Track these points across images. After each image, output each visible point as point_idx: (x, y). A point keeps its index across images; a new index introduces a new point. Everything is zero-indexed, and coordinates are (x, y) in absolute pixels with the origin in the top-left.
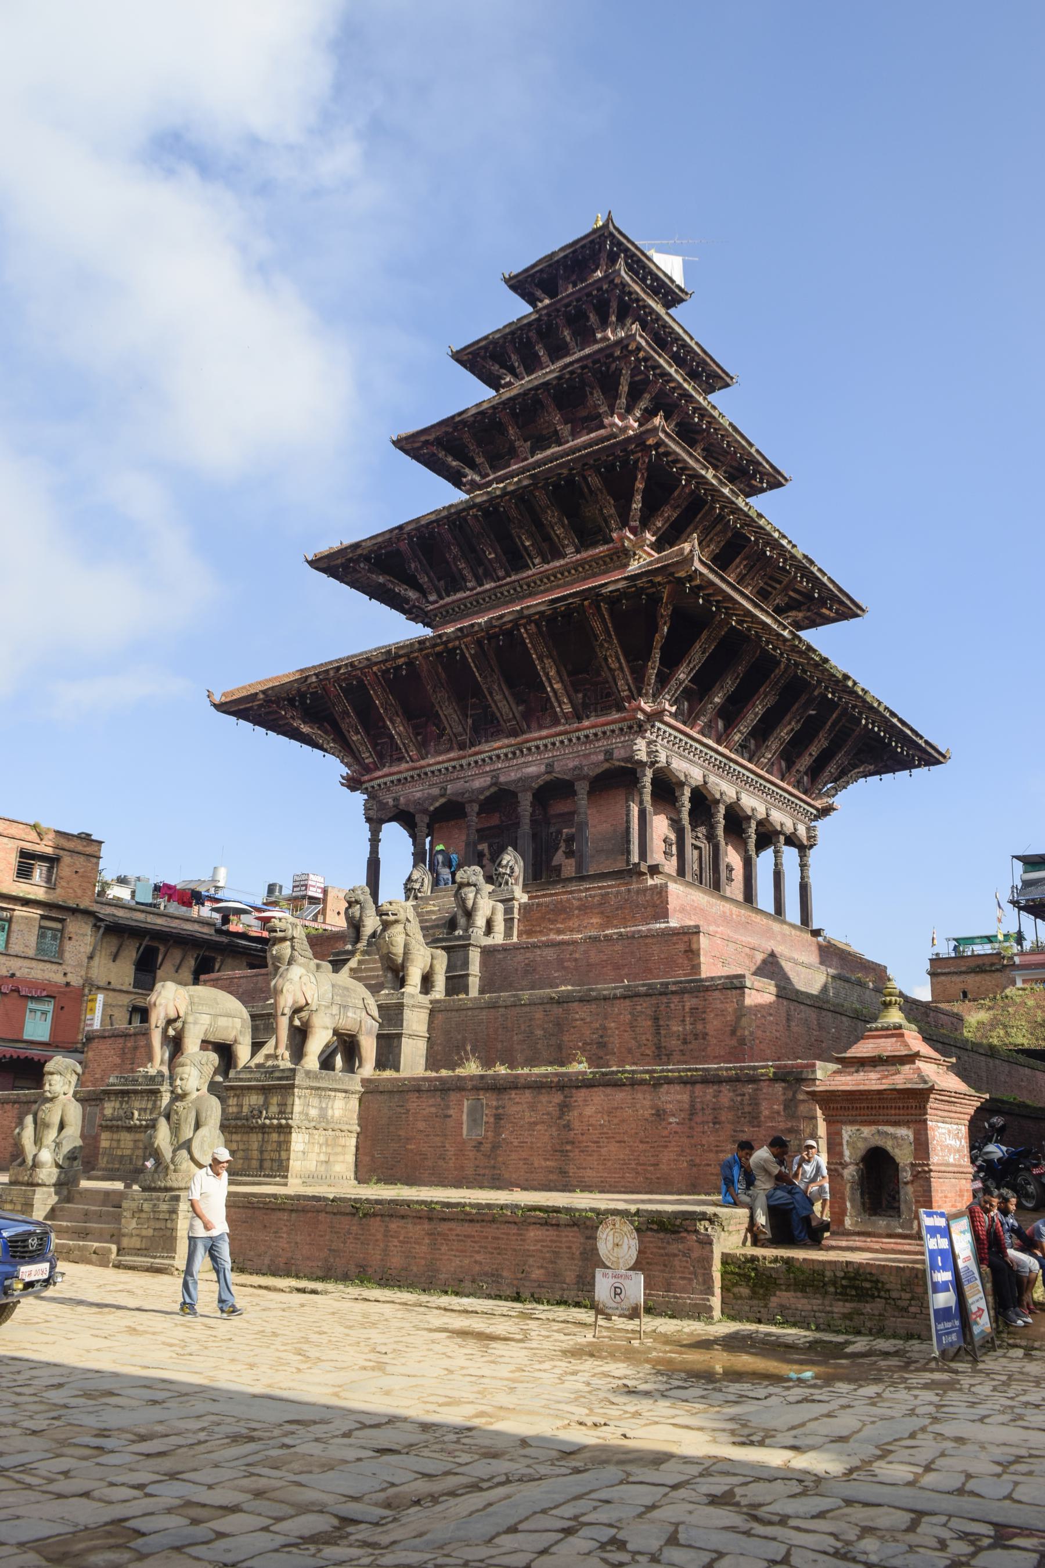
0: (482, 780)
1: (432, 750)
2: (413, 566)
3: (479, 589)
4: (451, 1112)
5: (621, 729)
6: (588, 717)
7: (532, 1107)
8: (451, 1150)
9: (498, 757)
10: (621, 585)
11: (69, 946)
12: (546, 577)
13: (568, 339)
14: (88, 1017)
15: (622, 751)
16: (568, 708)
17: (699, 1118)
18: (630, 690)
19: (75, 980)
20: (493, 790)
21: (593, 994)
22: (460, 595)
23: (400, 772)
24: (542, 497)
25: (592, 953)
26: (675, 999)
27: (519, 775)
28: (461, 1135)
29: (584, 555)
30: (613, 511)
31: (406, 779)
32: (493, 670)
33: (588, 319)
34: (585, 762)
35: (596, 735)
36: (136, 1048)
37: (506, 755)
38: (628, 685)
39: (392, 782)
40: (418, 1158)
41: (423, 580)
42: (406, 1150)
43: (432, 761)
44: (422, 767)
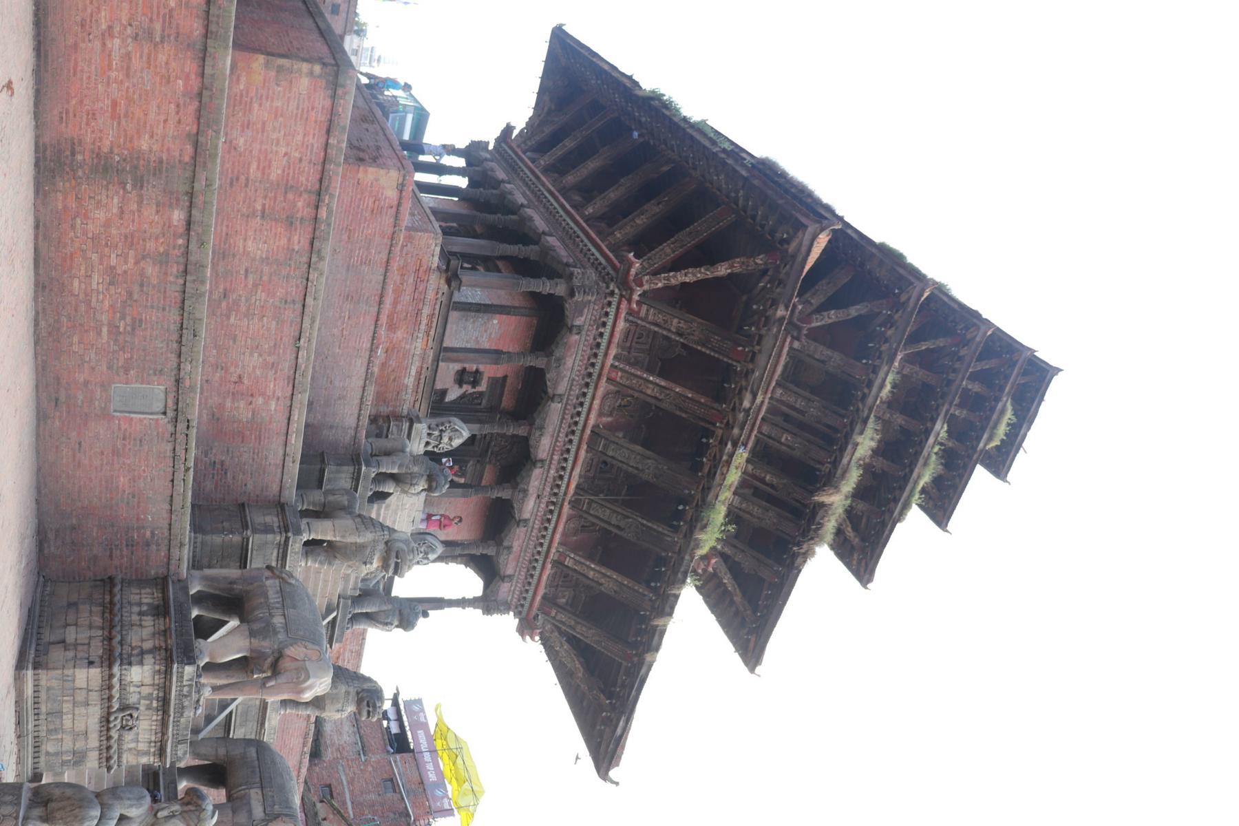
5: (525, 598)
9: (561, 477)
10: (619, 731)
18: (554, 618)
23: (606, 354)
27: (531, 490)
31: (595, 355)
34: (511, 557)
35: (532, 576)
36: (290, 222)
37: (558, 486)
38: (562, 622)
39: (601, 335)
41: (821, 351)
43: (597, 403)
44: (596, 388)
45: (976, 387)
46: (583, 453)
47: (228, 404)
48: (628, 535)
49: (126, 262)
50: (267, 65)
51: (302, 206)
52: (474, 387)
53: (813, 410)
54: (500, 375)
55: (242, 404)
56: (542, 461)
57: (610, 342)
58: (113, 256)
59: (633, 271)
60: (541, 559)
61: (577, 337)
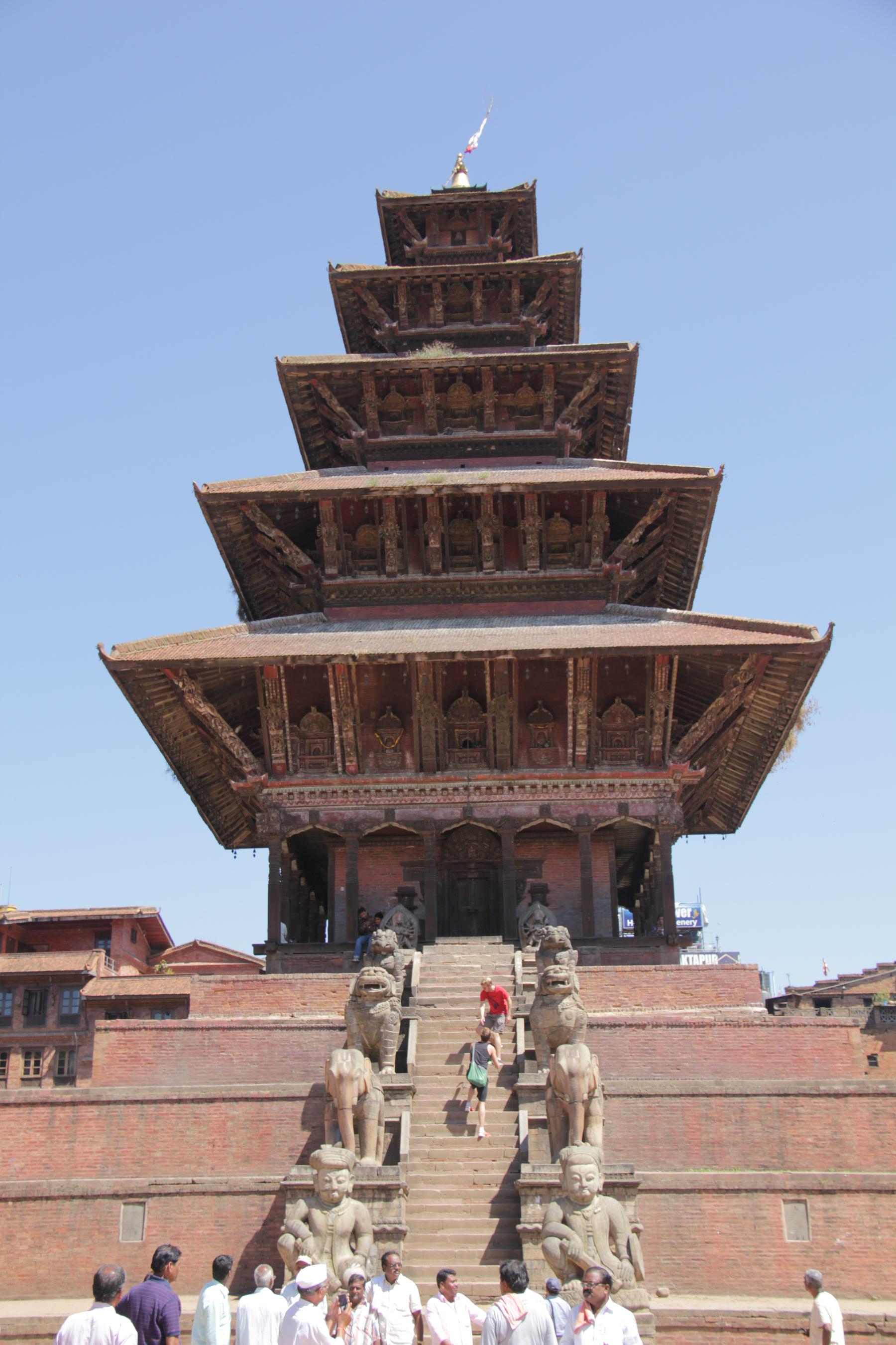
0: (449, 810)
1: (371, 765)
2: (324, 530)
3: (401, 577)
4: (765, 1213)
5: (644, 785)
9: (478, 788)
12: (500, 585)
13: (478, 304)
15: (640, 809)
16: (582, 751)
20: (464, 823)
21: (822, 1088)
22: (369, 577)
24: (531, 506)
27: (502, 813)
28: (782, 1239)
29: (554, 573)
30: (602, 538)
31: (334, 792)
32: (511, 696)
33: (509, 294)
35: (611, 785)
37: (489, 788)
39: (312, 793)
40: (724, 1265)
41: (329, 548)
42: (706, 1255)
45: (402, 304)
47: (234, 1150)
48: (512, 703)
49: (26, 1239)
51: (62, 1113)
52: (416, 894)
53: (390, 527)
54: (401, 870)
55: (233, 1139)
56: (465, 810)
57: (316, 784)
58: (21, 1248)
59: (241, 784)
60: (584, 782)
61: (321, 814)
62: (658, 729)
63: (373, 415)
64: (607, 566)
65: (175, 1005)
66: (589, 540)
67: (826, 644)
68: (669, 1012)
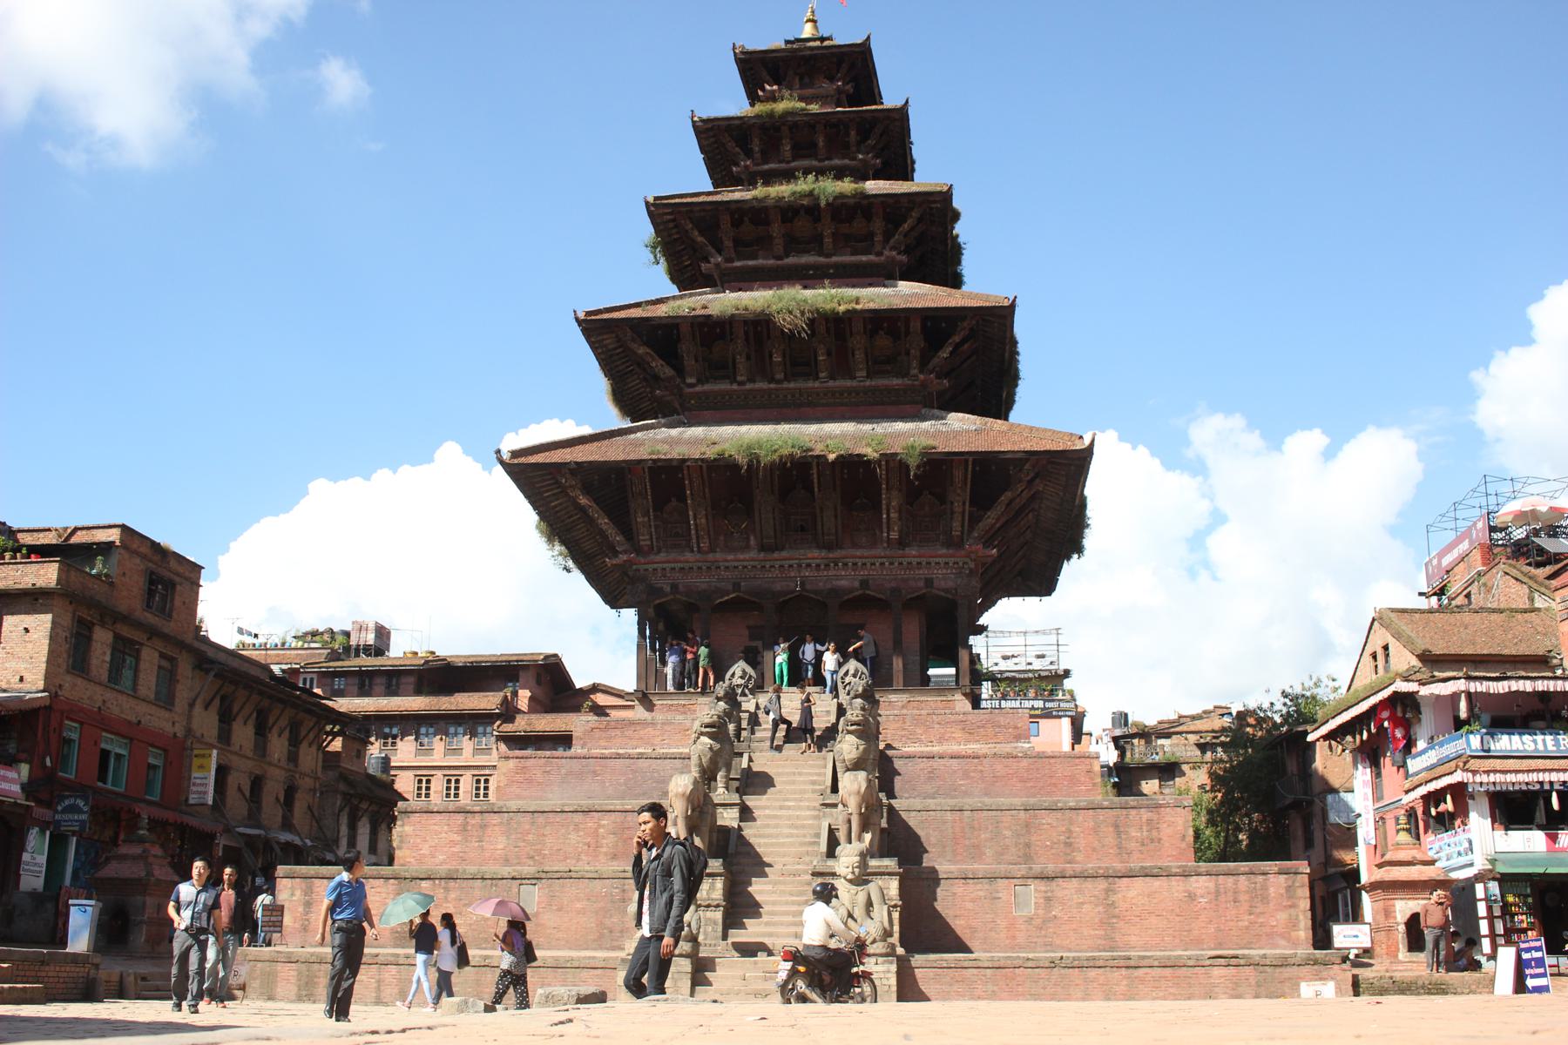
3: (749, 386)
6: (909, 545)
7: (1079, 891)
8: (1002, 923)
9: (809, 565)
11: (179, 687)
13: (821, 144)
14: (194, 774)
16: (894, 535)
17: (1222, 898)
19: (179, 731)
22: (723, 386)
25: (999, 767)
26: (1133, 812)
33: (848, 135)
37: (818, 566)
46: (784, 554)
50: (400, 848)
62: (957, 517)
63: (728, 243)
64: (922, 377)
65: (564, 740)
66: (908, 354)
67: (1089, 451)
68: (954, 748)
